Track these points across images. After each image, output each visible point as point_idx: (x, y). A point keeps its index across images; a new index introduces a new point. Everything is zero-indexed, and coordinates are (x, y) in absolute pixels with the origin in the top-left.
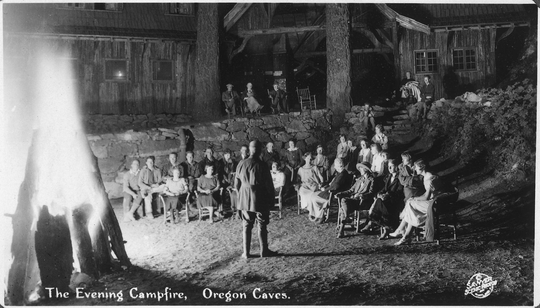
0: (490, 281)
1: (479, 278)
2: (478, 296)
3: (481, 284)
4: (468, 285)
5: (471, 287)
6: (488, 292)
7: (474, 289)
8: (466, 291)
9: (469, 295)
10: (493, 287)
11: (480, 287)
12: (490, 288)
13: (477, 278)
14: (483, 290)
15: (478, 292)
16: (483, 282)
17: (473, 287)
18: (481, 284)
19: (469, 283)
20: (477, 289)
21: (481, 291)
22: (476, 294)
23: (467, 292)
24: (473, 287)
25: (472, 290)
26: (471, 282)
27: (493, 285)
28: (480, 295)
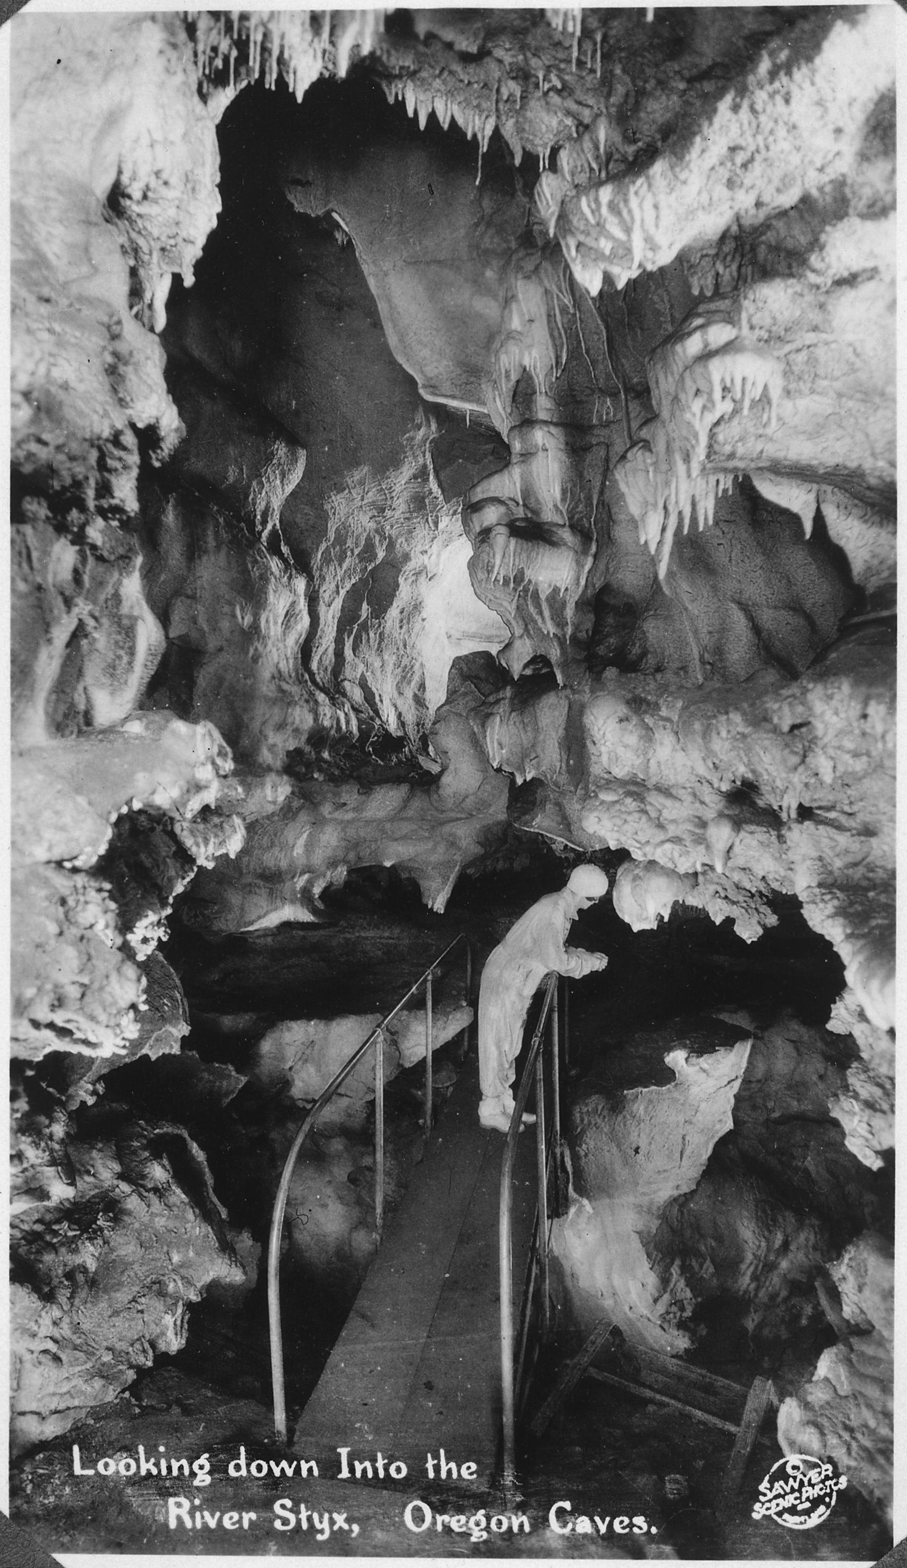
2: (791, 1522)
3: (802, 1484)
4: (762, 1488)
5: (770, 1495)
6: (822, 1509)
7: (780, 1500)
8: (757, 1506)
9: (767, 1518)
11: (797, 1494)
12: (827, 1499)
13: (789, 1470)
14: (808, 1505)
16: (806, 1480)
17: (776, 1497)
19: (764, 1486)
20: (790, 1500)
21: (800, 1508)
23: (758, 1512)
24: (776, 1497)
27: (835, 1488)
28: (797, 1519)
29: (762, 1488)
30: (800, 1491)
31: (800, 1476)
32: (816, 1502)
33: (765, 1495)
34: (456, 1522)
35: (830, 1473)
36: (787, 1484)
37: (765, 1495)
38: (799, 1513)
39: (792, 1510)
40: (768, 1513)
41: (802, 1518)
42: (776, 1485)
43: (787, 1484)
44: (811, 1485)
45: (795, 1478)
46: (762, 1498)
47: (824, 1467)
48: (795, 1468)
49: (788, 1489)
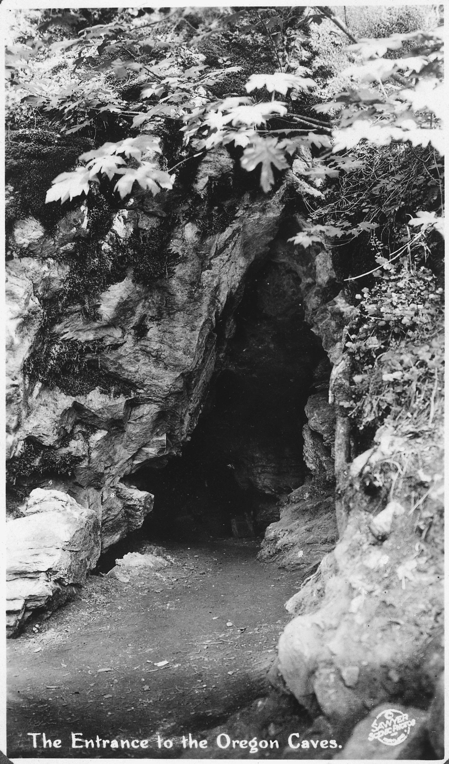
0: (405, 721)
1: (389, 715)
3: (393, 723)
4: (373, 726)
5: (377, 729)
7: (382, 731)
8: (371, 734)
11: (390, 728)
12: (405, 731)
13: (386, 716)
14: (396, 734)
17: (380, 730)
18: (393, 723)
20: (387, 732)
21: (392, 735)
22: (385, 739)
24: (380, 730)
27: (410, 725)
28: (390, 740)
30: (392, 726)
34: (242, 744)
35: (407, 718)
36: (385, 723)
38: (393, 737)
39: (389, 736)
40: (376, 738)
41: (394, 740)
43: (385, 723)
44: (397, 724)
46: (373, 730)
47: (404, 715)
48: (389, 715)
49: (386, 726)
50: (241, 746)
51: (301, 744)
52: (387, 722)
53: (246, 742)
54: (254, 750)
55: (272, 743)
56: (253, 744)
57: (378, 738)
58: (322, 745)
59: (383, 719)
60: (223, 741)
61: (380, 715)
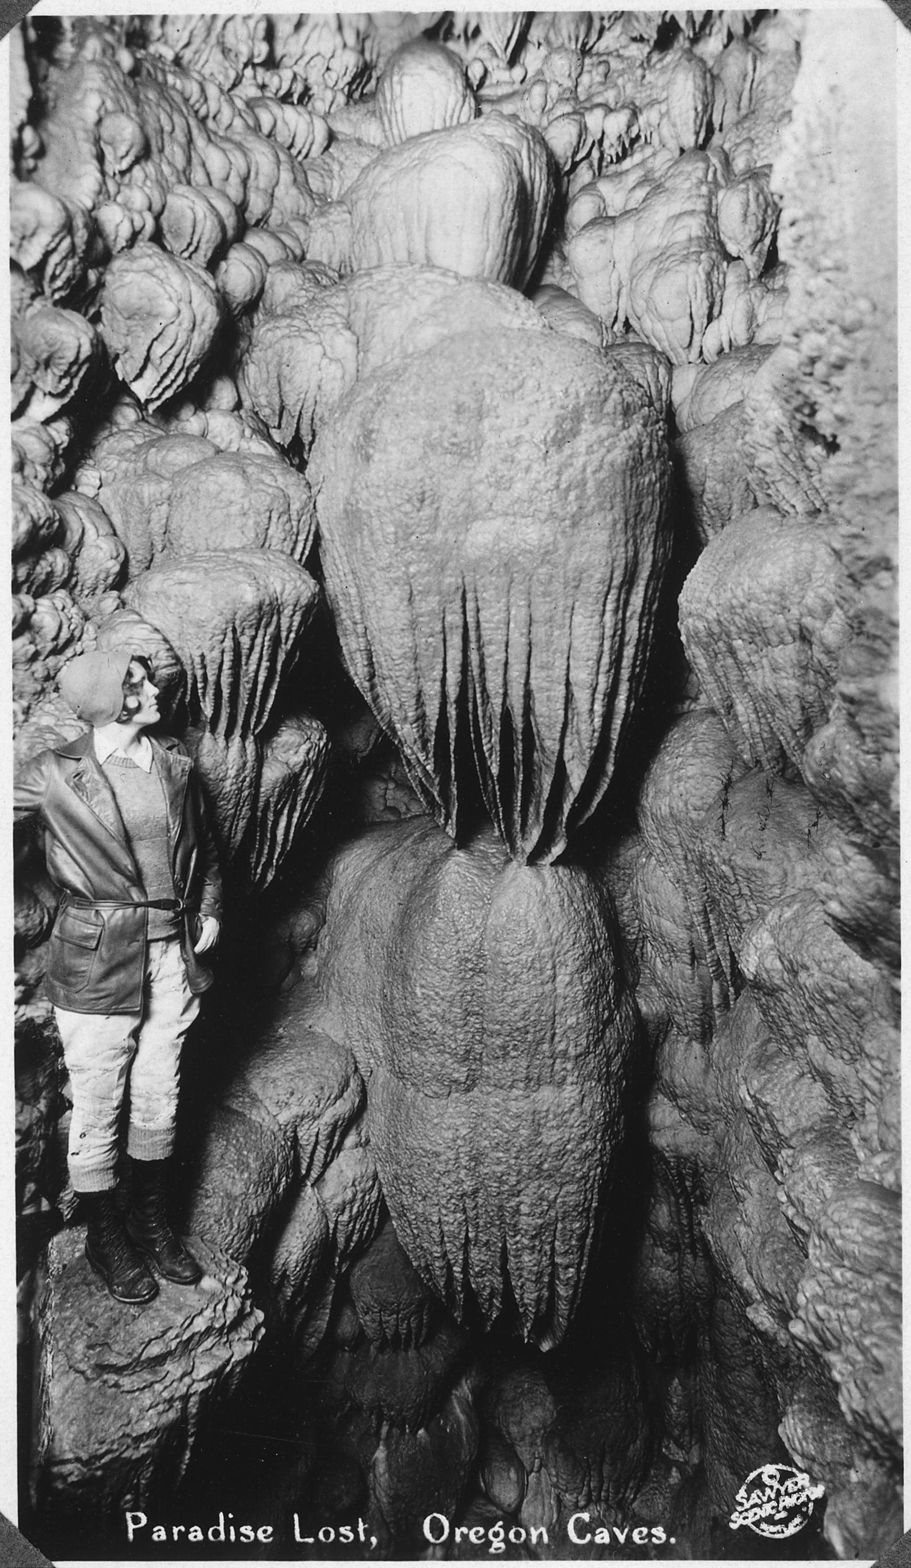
2: (768, 1531)
3: (778, 1493)
4: (738, 1498)
5: (747, 1506)
6: (797, 1520)
7: (756, 1510)
9: (743, 1528)
10: (811, 1505)
13: (765, 1479)
14: (783, 1515)
15: (770, 1520)
16: (783, 1489)
17: (753, 1507)
19: (742, 1493)
20: (767, 1510)
22: (764, 1526)
23: (737, 1521)
24: (753, 1507)
25: (750, 1514)
26: (749, 1492)
28: (773, 1529)
29: (738, 1498)
31: (776, 1485)
32: (793, 1512)
33: (742, 1504)
37: (742, 1504)
39: (770, 1520)
41: (779, 1528)
42: (754, 1495)
45: (771, 1487)
46: (739, 1509)
48: (771, 1477)
49: (765, 1499)
50: (473, 1538)
51: (594, 1535)
52: (768, 1490)
53: (482, 1531)
54: (498, 1544)
55: (534, 1534)
56: (496, 1535)
57: (748, 1522)
58: (636, 1537)
59: (758, 1484)
60: (437, 1528)
61: (752, 1475)
